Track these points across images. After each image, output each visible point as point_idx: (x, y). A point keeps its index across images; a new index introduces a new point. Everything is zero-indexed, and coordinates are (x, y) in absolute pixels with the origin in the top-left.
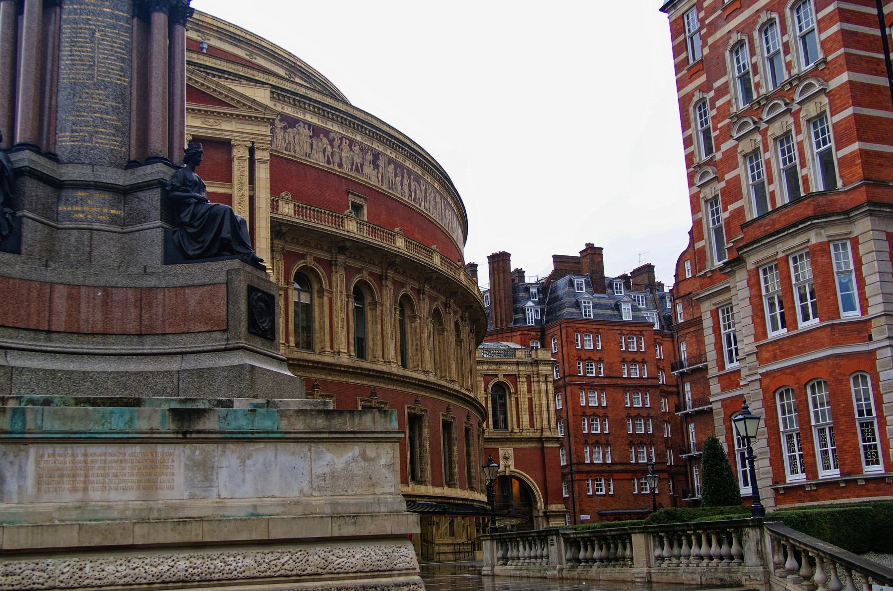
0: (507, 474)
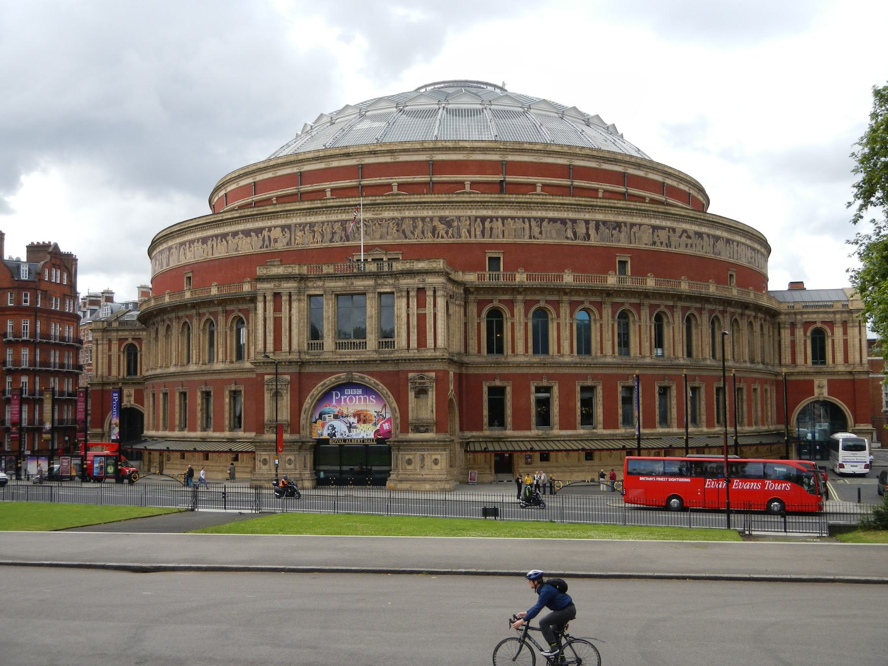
0: (821, 399)
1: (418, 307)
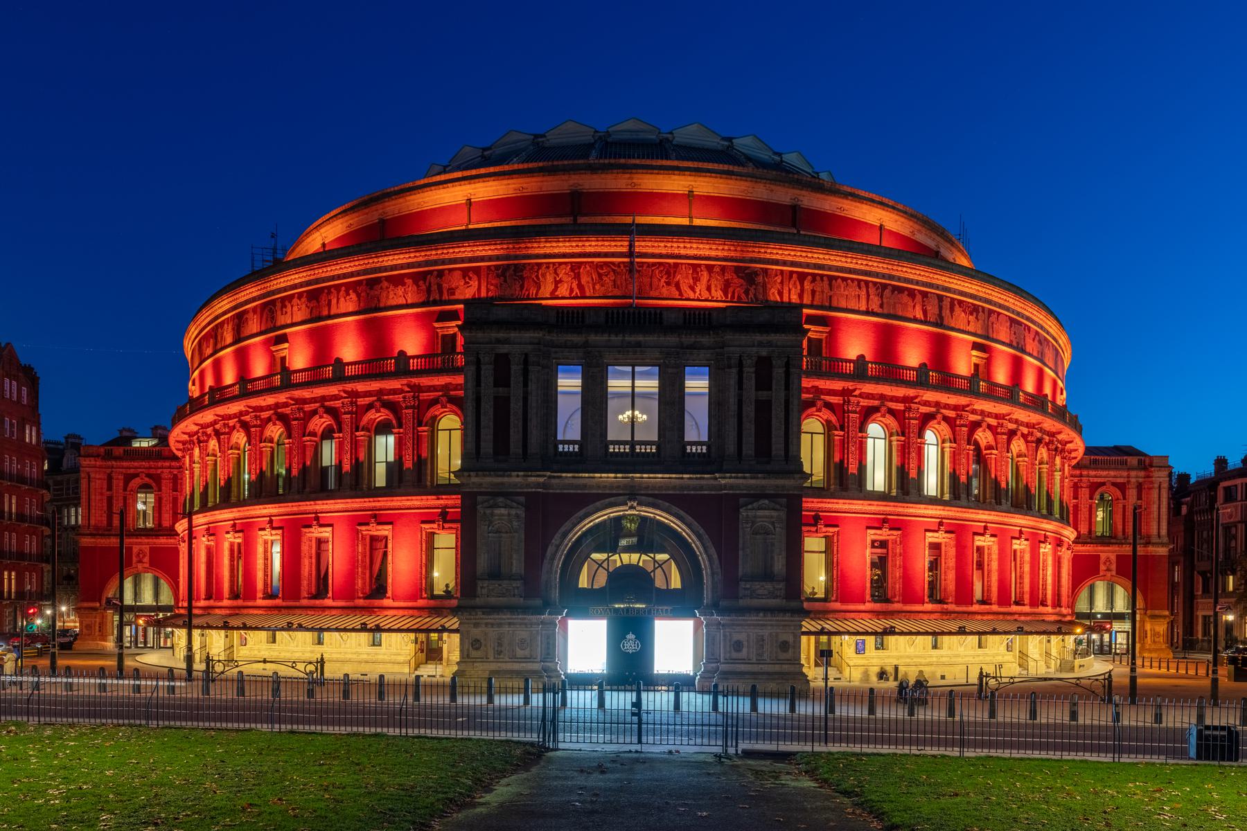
1: (757, 389)
